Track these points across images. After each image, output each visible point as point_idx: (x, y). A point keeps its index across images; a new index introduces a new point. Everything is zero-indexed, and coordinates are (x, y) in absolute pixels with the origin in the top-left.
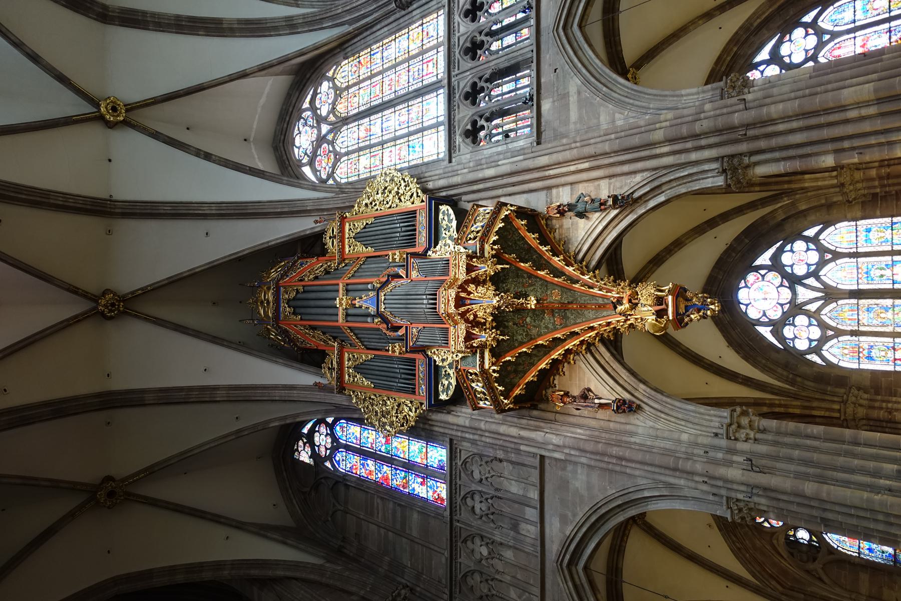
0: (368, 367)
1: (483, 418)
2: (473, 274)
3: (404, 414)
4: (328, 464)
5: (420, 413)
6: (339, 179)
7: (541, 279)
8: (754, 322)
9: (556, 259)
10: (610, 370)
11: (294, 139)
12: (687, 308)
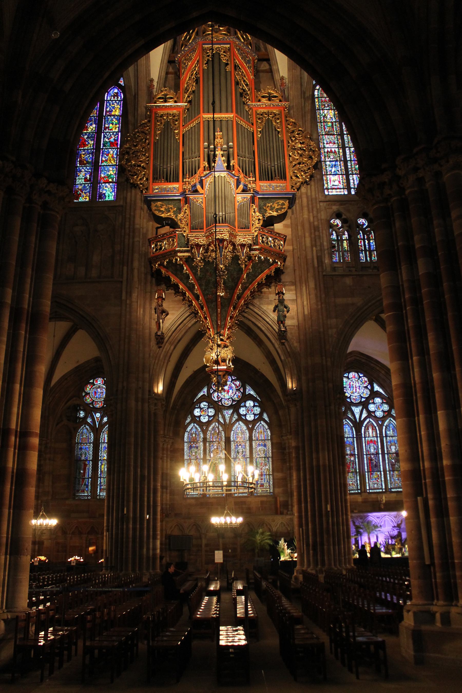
1: (141, 237)
3: (137, 172)
8: (210, 385)
9: (249, 293)
10: (180, 326)
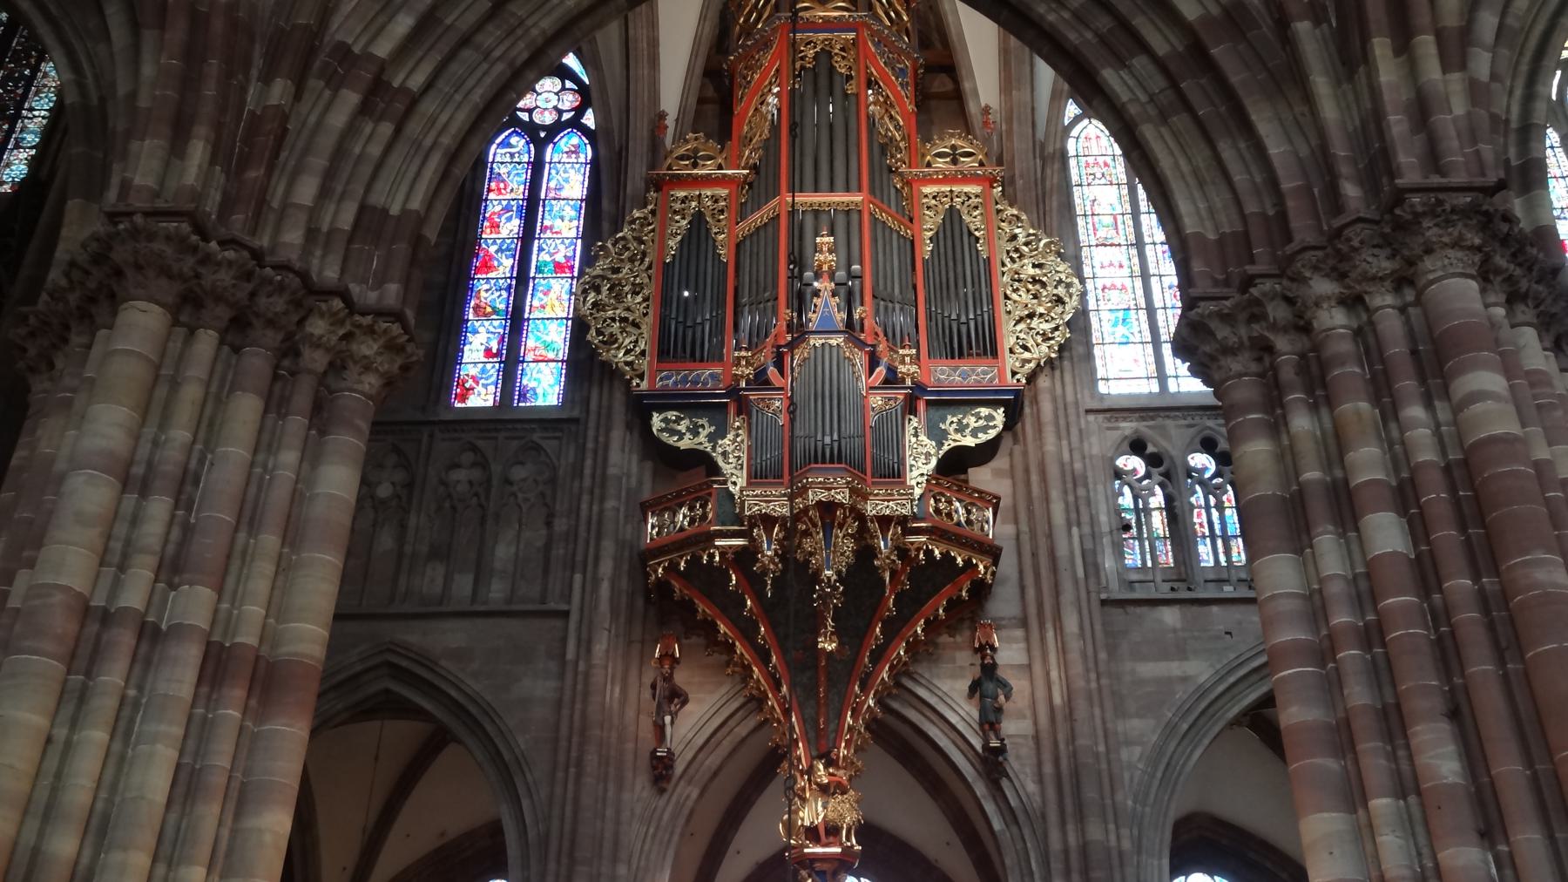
0: (703, 246)
2: (874, 526)
3: (619, 336)
5: (623, 374)
6: (1075, 132)
10: (719, 735)
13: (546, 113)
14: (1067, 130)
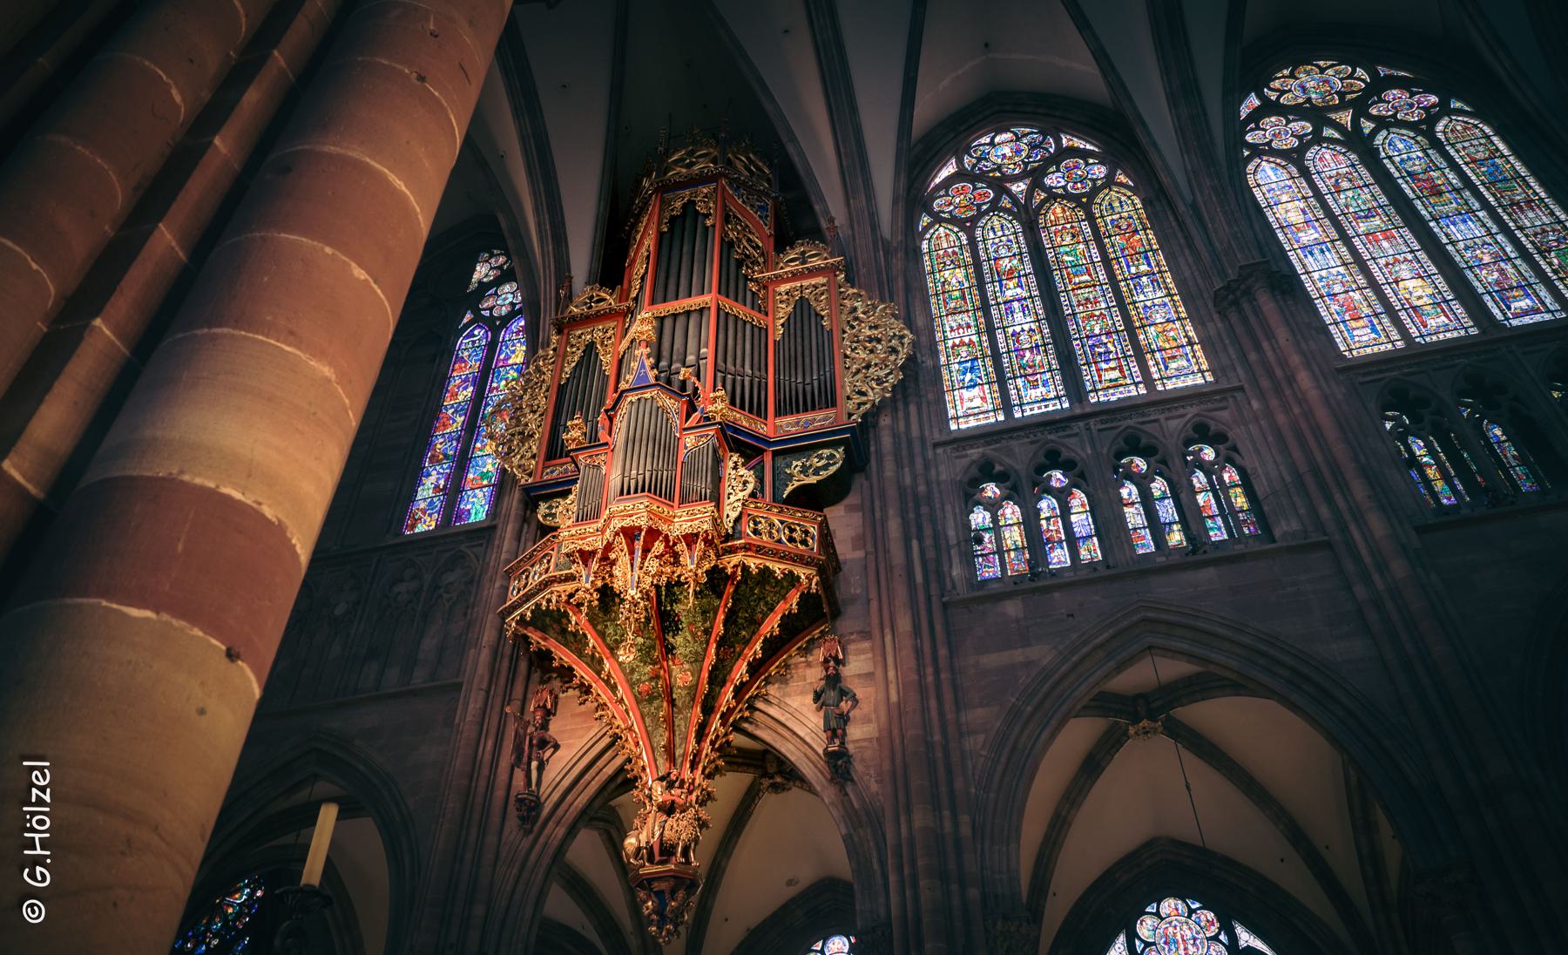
4: (468, 317)
6: (928, 236)
7: (706, 650)
9: (744, 668)
10: (588, 777)
11: (1007, 130)
12: (660, 894)
13: (504, 308)
14: (921, 236)
